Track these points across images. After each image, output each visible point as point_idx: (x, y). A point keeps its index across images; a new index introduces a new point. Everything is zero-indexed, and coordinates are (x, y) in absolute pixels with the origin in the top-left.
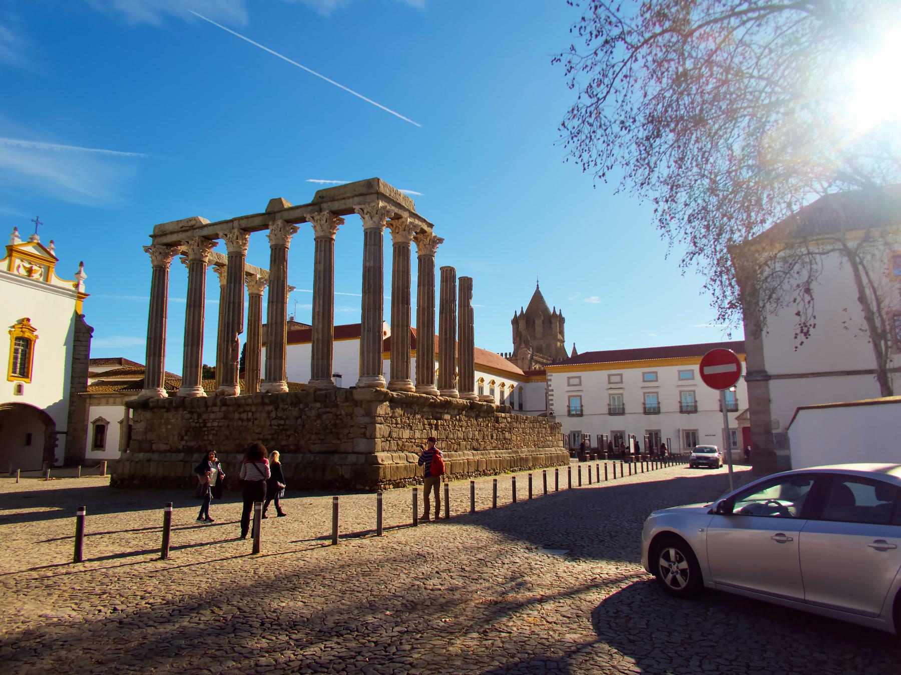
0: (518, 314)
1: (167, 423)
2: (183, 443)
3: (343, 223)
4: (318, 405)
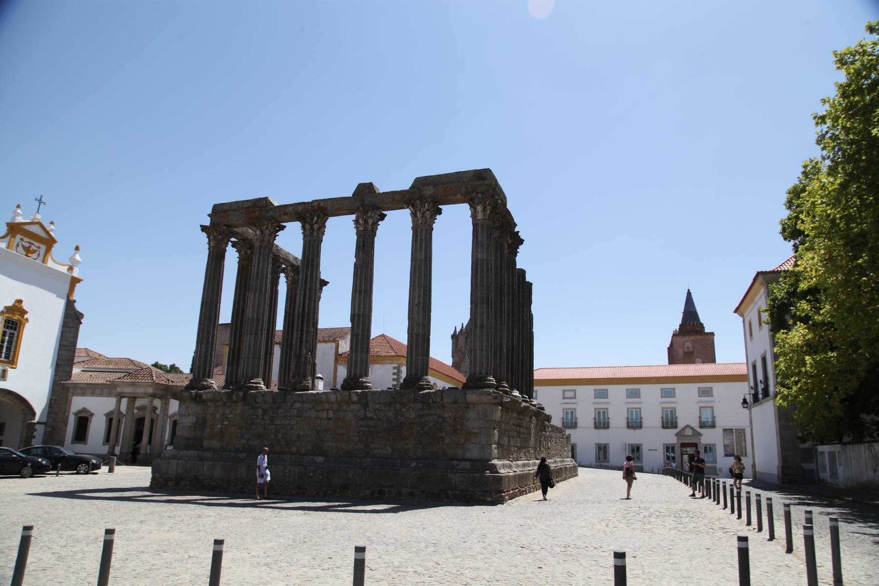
0: (458, 330)
1: (224, 417)
2: (243, 441)
3: (440, 213)
4: (419, 406)
